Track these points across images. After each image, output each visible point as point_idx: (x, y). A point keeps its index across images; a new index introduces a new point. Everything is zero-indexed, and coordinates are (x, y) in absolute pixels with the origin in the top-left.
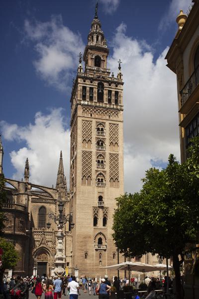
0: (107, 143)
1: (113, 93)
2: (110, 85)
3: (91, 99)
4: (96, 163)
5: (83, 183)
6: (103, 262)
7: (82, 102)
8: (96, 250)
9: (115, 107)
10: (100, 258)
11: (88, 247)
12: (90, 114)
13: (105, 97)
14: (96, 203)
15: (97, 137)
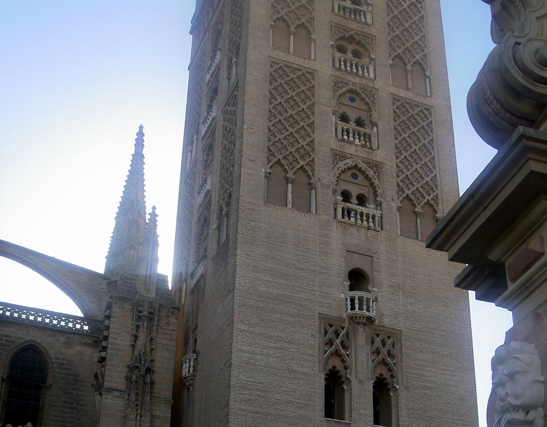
0: (381, 53)
5: (274, 197)
15: (336, 19)
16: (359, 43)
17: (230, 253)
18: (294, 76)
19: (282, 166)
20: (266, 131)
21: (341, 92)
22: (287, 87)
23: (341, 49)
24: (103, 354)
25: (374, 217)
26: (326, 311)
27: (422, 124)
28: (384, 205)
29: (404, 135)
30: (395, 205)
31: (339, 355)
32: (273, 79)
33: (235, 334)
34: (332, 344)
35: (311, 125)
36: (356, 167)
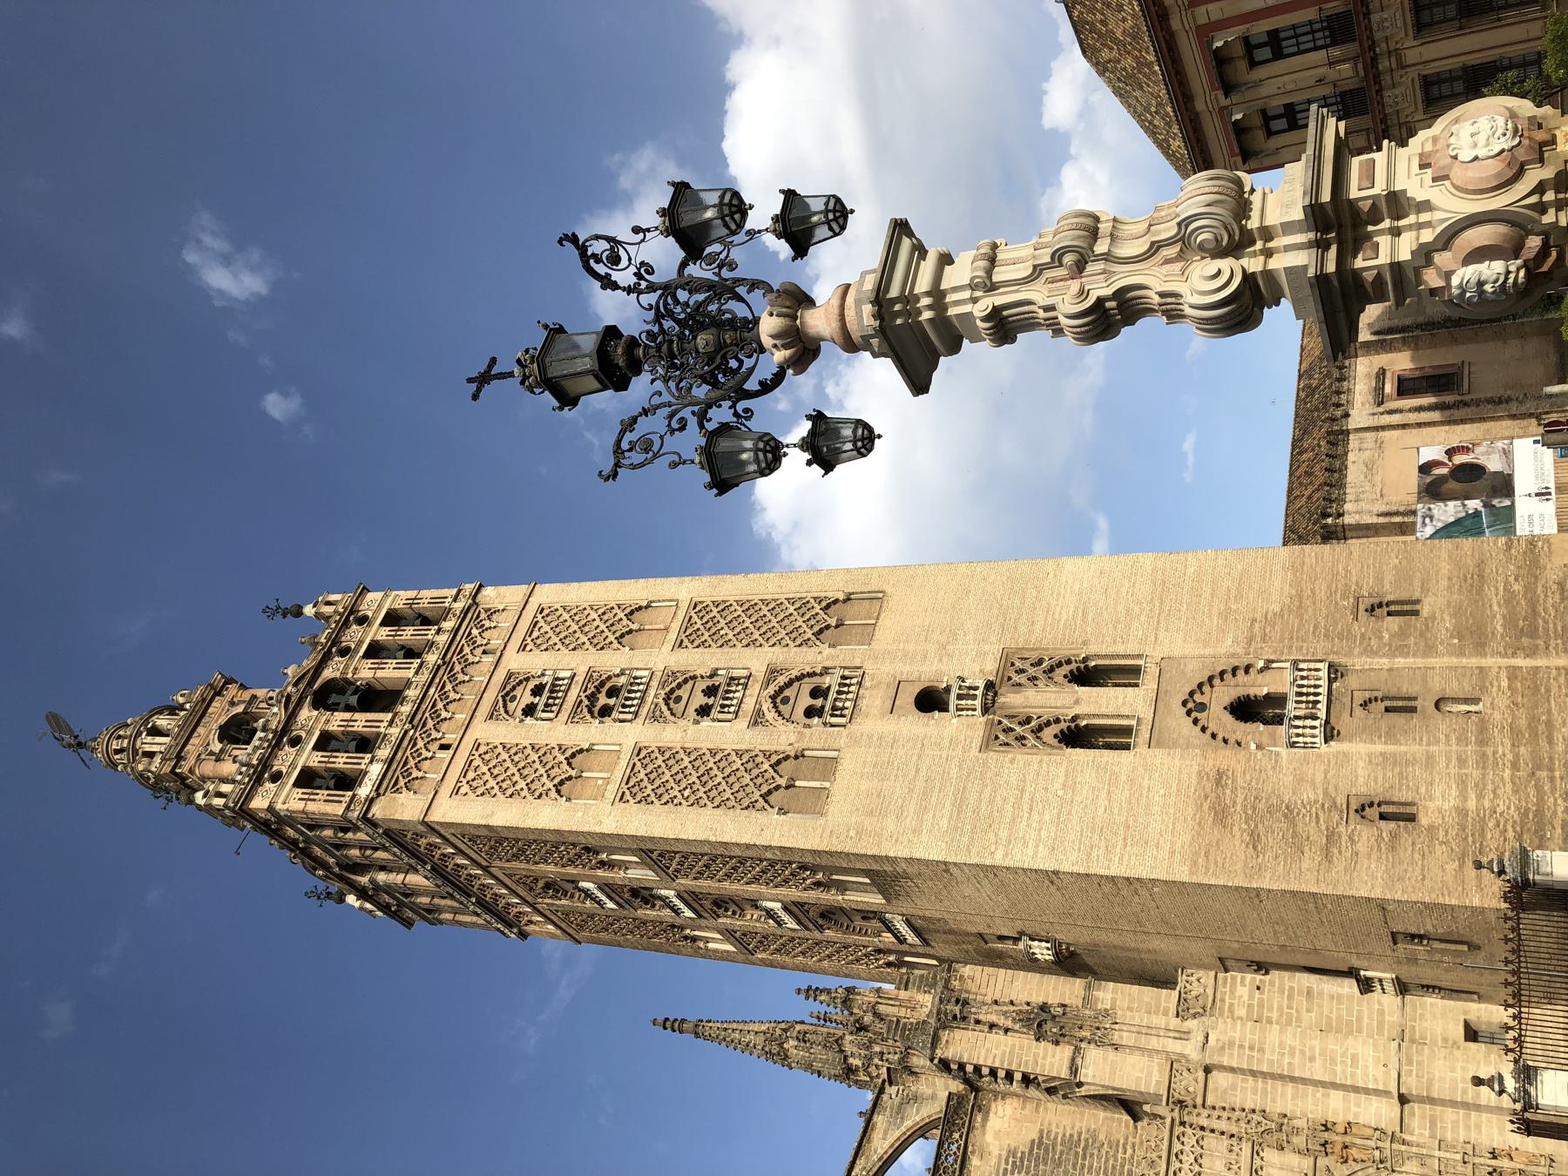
0: (612, 661)
1: (383, 634)
2: (344, 652)
3: (364, 744)
4: (706, 723)
5: (815, 803)
6: (1437, 686)
7: (364, 791)
8: (1330, 735)
9: (448, 625)
10: (1413, 710)
11: (1308, 794)
12: (442, 754)
13: (389, 672)
14: (960, 728)
15: (564, 716)
16: (598, 689)
17: (888, 868)
18: (643, 772)
19: (769, 792)
20: (719, 811)
21: (667, 713)
22: (658, 782)
23: (605, 712)
24: (1018, 1076)
25: (844, 677)
26: (977, 742)
27: (715, 613)
28: (828, 664)
29: (730, 636)
30: (827, 651)
31: (1040, 728)
32: (645, 800)
33: (1011, 864)
34: (1024, 738)
35: (713, 753)
36: (773, 698)
